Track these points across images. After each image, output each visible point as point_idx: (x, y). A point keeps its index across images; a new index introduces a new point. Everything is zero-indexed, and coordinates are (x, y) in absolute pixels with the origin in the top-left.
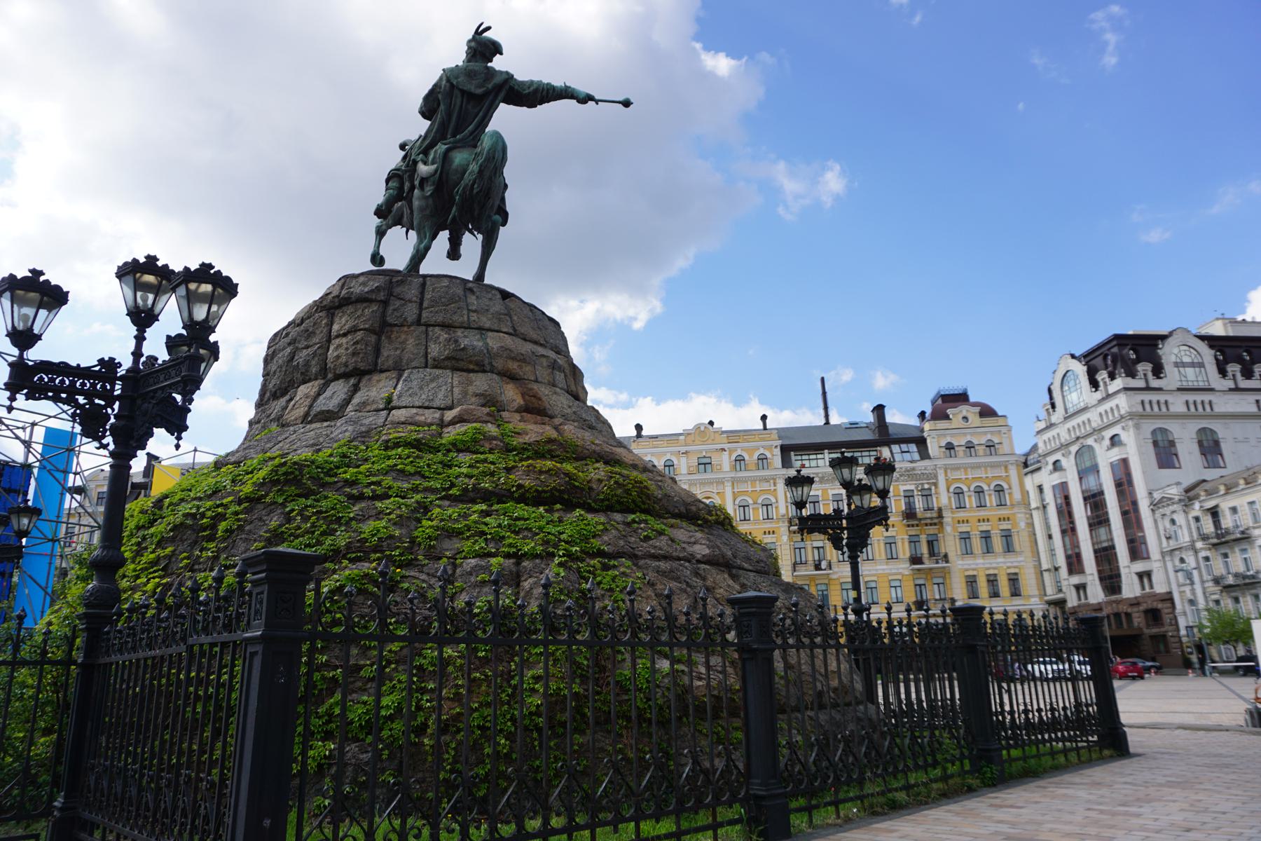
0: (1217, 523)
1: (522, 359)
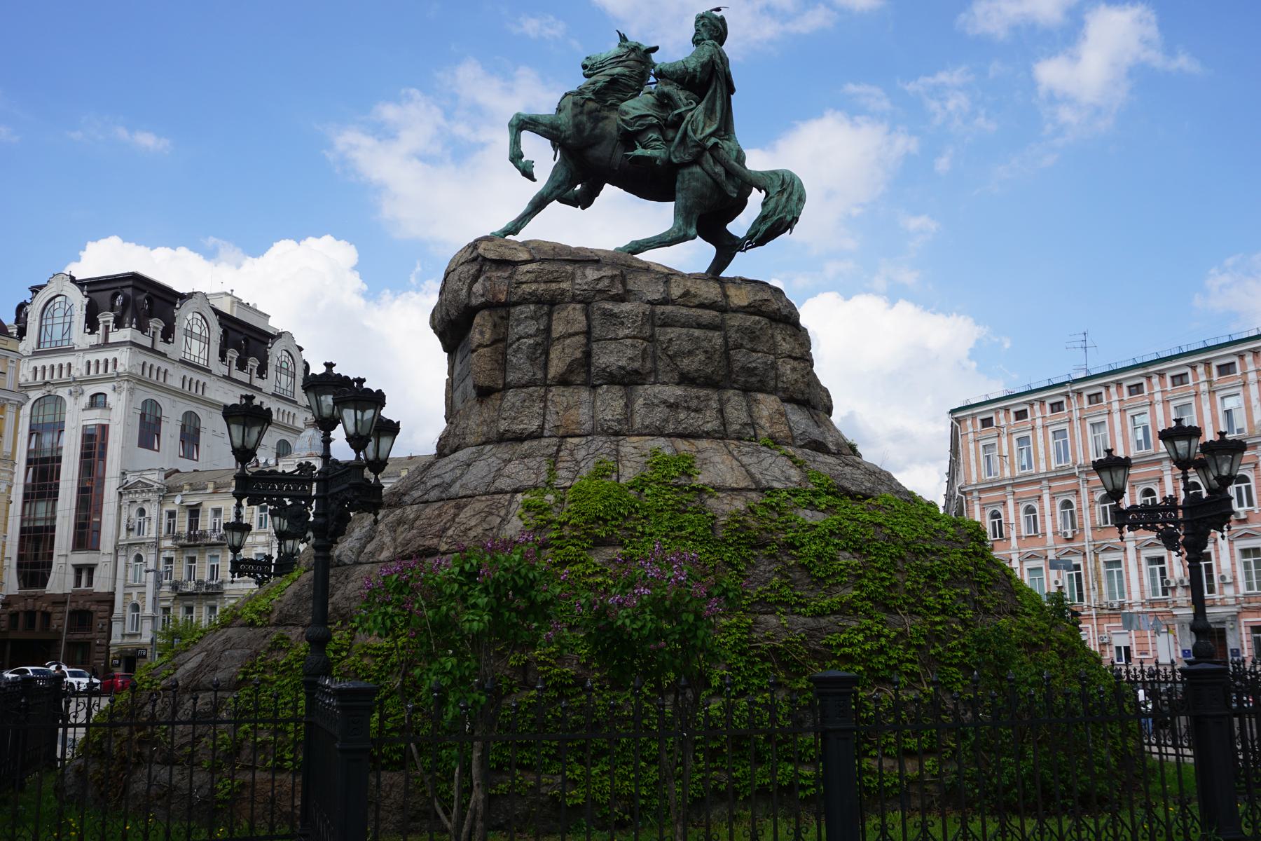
0: (193, 523)
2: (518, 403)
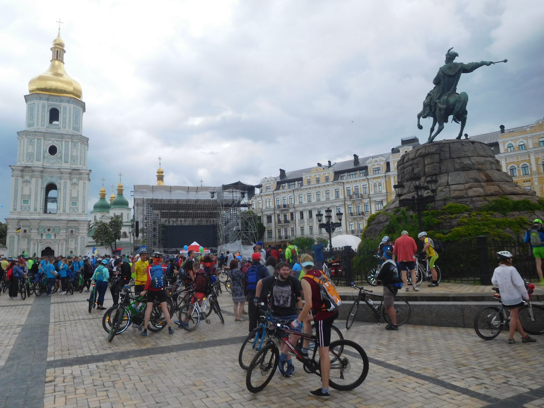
1: (482, 164)
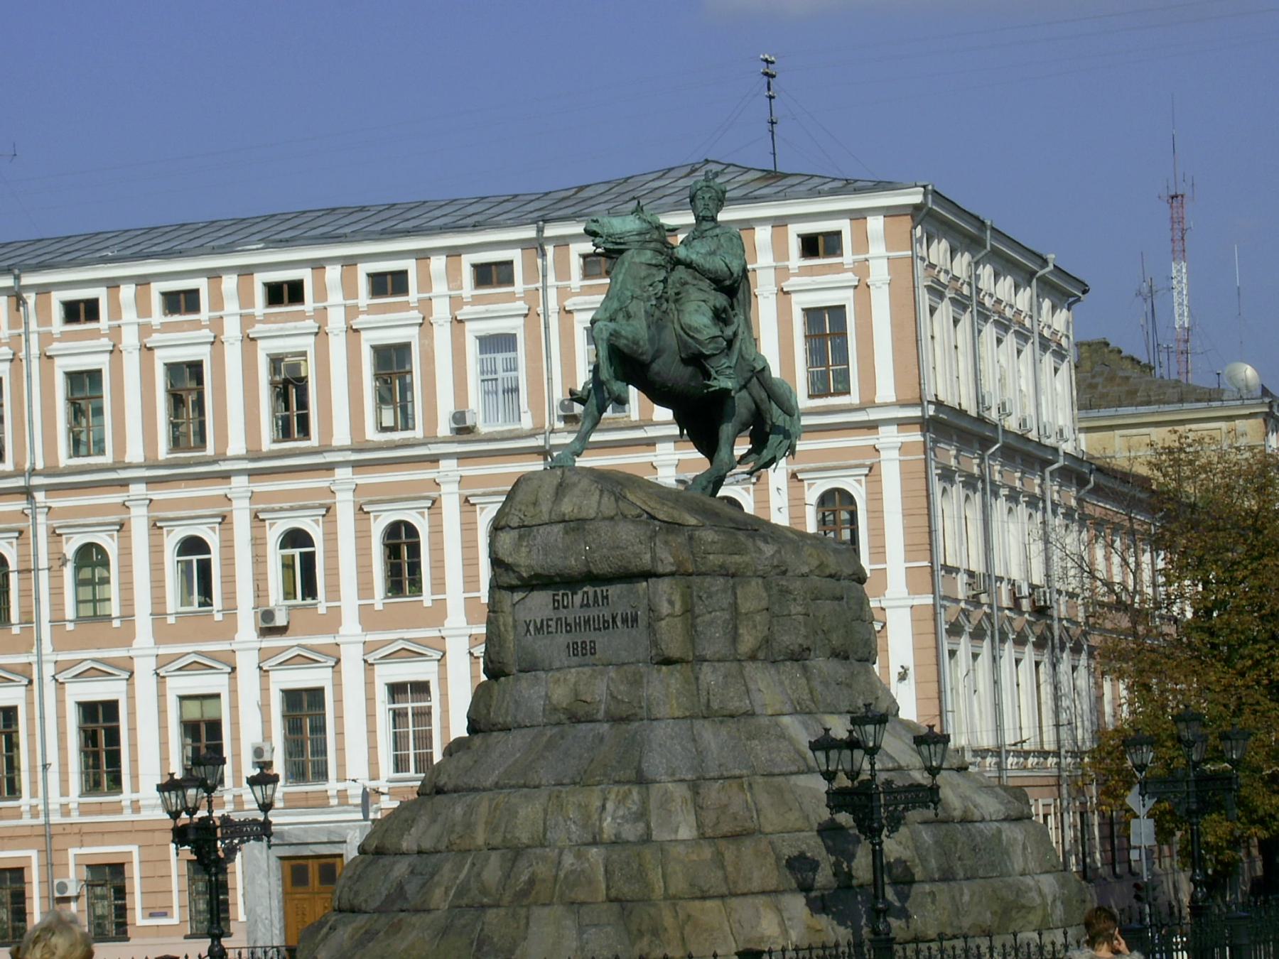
2: (721, 678)
